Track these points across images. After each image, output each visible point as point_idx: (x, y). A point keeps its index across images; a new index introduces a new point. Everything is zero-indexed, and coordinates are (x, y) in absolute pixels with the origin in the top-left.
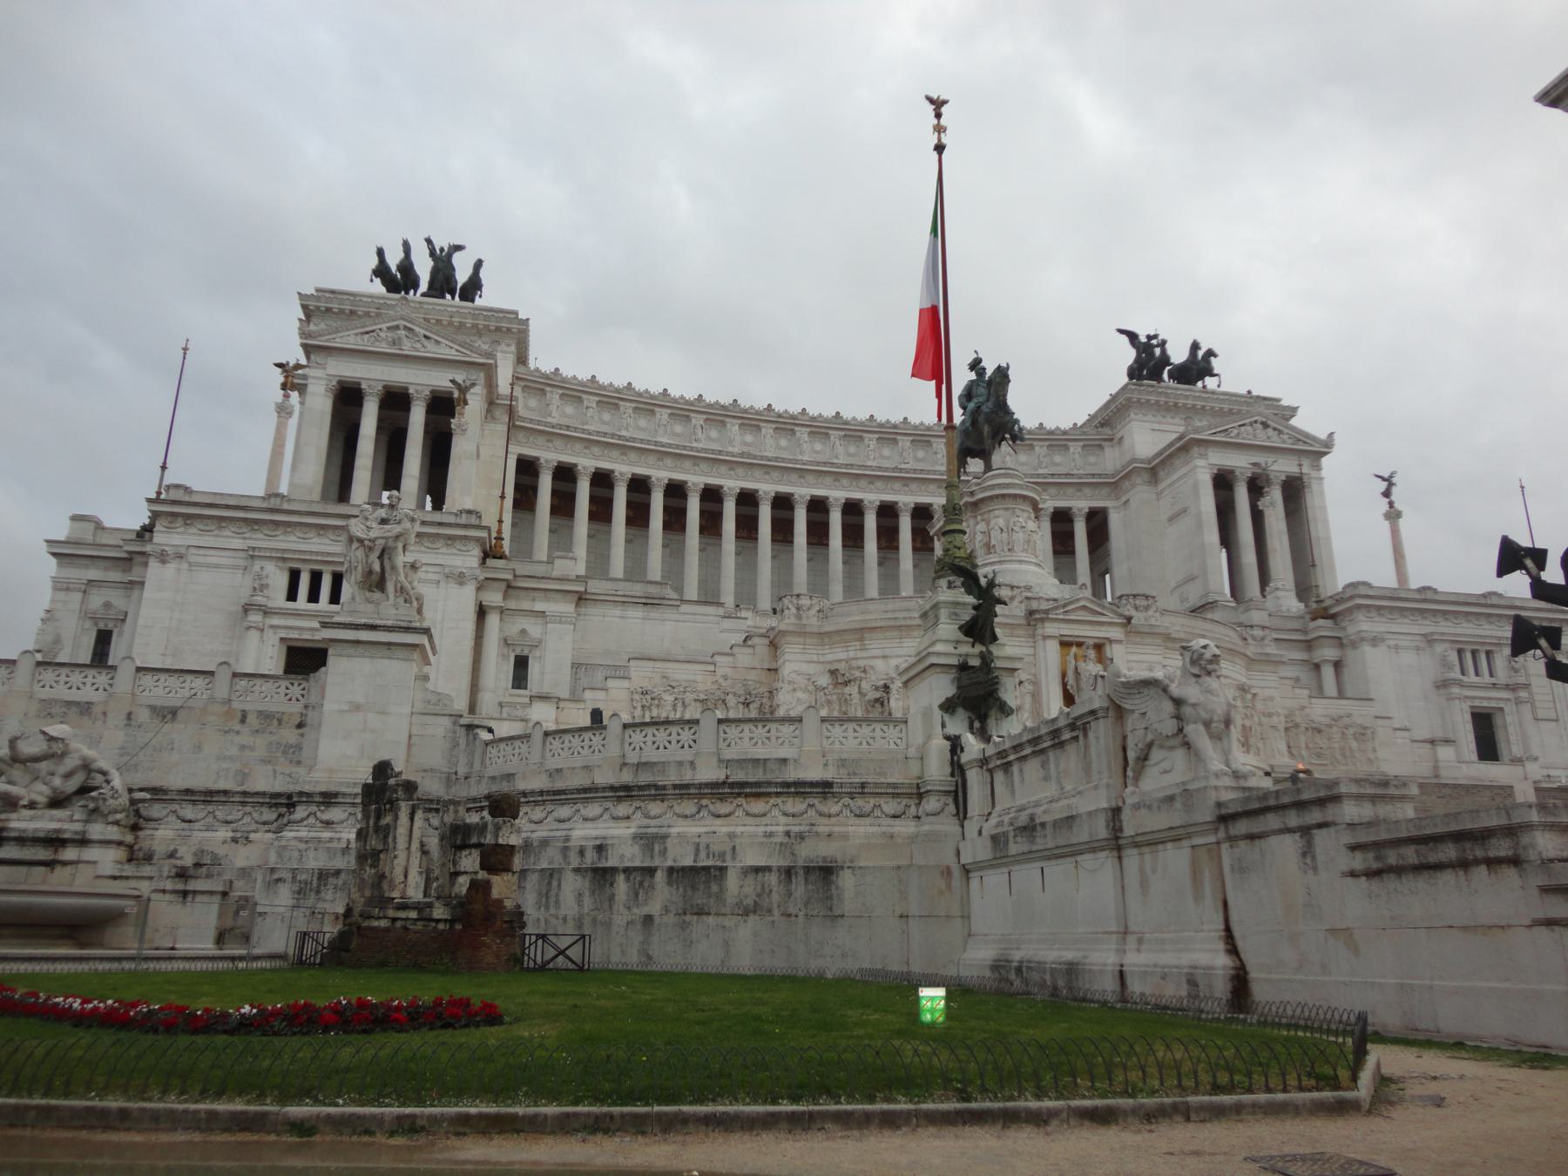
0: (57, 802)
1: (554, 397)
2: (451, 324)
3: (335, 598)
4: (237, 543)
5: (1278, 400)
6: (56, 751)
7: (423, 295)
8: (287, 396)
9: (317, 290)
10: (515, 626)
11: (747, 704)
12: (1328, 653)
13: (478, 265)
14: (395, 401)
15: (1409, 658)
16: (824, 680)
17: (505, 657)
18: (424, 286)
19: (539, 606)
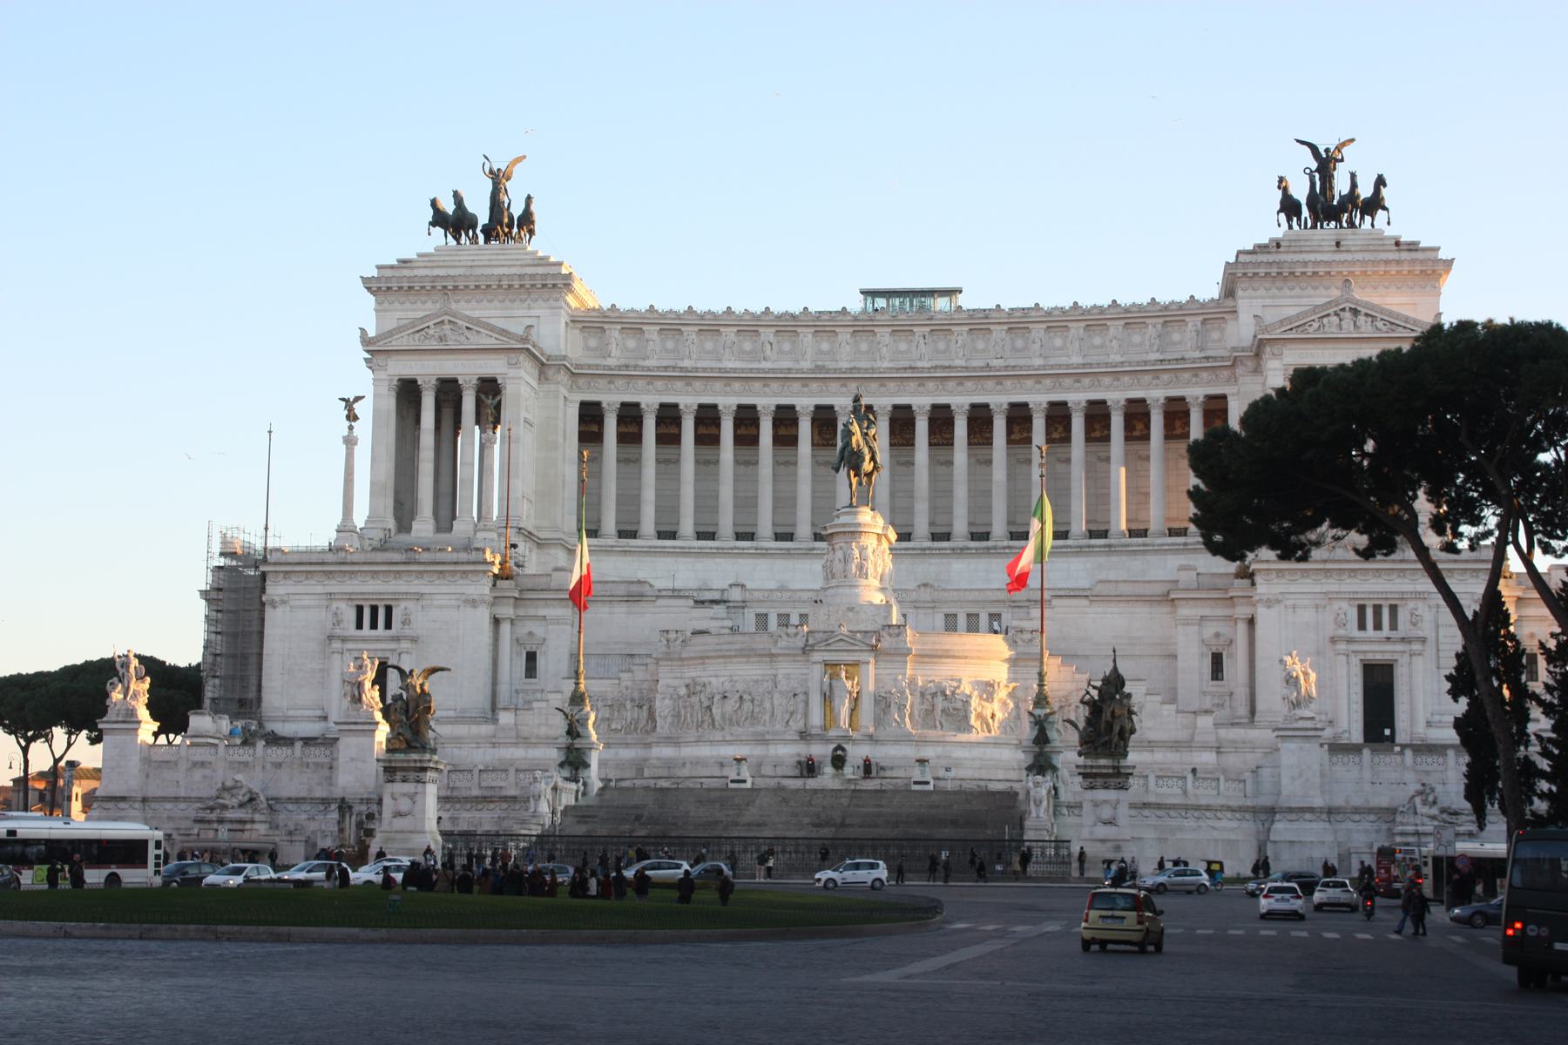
0: (241, 805)
1: (614, 333)
2: (500, 286)
3: (388, 626)
4: (319, 589)
5: (1437, 249)
6: (237, 786)
7: (486, 230)
8: (351, 428)
9: (379, 267)
10: (523, 629)
11: (641, 707)
12: (1242, 611)
13: (529, 199)
14: (449, 391)
15: (1307, 616)
16: (683, 691)
17: (519, 654)
18: (483, 218)
19: (542, 612)
